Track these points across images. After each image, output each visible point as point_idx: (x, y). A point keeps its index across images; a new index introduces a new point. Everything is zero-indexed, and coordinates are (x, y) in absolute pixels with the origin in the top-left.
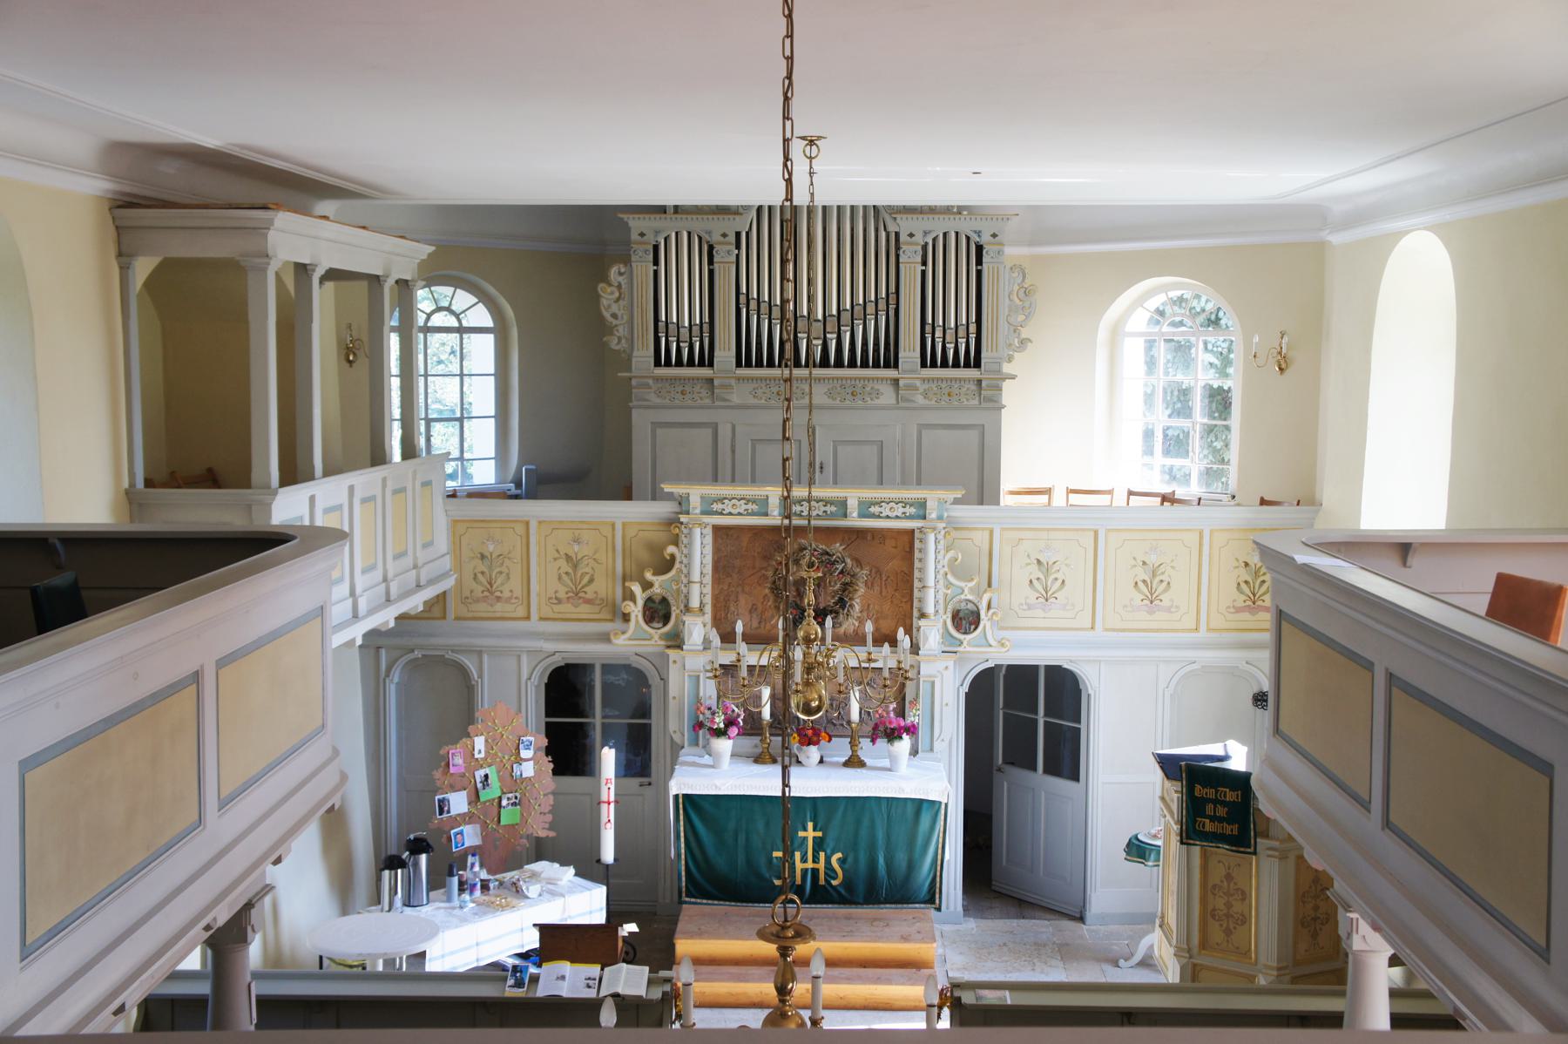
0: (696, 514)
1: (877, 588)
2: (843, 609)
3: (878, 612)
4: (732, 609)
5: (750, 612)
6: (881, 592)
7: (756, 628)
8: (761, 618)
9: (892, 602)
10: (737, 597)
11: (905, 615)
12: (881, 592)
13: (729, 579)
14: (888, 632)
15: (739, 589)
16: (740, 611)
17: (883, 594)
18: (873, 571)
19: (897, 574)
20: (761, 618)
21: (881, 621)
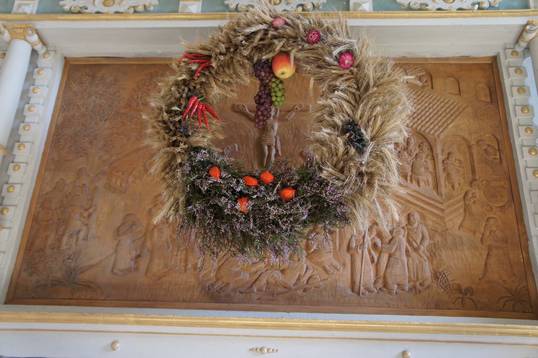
0: (25, 13)
1: (426, 177)
2: (361, 152)
3: (433, 232)
4: (77, 223)
5: (118, 232)
6: (437, 186)
7: (129, 270)
8: (143, 246)
9: (467, 208)
10: (92, 199)
11: (506, 241)
12: (437, 186)
13: (81, 160)
14: (465, 283)
15: (101, 184)
16: (93, 231)
17: (444, 190)
18: (412, 141)
19: (470, 147)
20: (143, 246)
21: (444, 255)
